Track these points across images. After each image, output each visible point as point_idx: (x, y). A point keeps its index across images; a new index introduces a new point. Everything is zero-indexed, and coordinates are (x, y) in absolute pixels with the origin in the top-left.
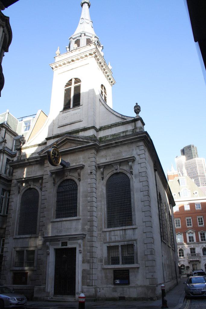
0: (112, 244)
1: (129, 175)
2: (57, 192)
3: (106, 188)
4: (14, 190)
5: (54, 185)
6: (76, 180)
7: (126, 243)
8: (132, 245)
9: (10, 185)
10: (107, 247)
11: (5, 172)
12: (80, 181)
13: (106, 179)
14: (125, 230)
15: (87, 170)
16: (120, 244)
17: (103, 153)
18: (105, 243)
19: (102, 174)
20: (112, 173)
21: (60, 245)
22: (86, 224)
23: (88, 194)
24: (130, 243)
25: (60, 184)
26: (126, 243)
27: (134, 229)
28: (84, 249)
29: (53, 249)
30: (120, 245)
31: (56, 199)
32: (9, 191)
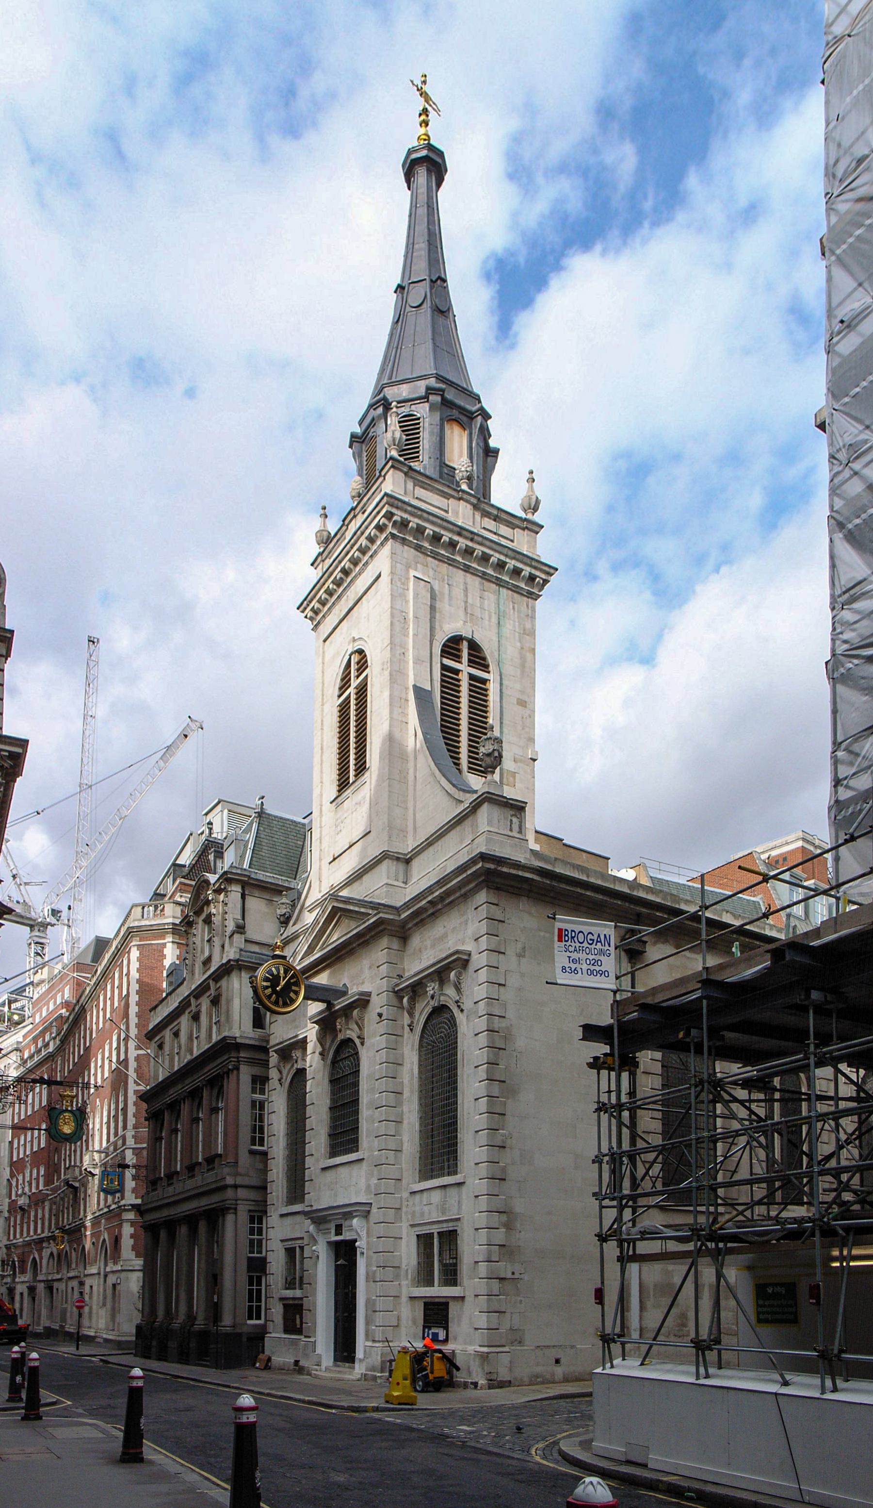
0: (425, 1230)
1: (455, 1010)
2: (331, 1081)
3: (420, 1060)
4: (273, 1074)
5: (323, 1059)
6: (357, 1041)
7: (445, 1225)
8: (456, 1231)
9: (265, 1064)
10: (418, 1236)
11: (258, 1022)
12: (362, 1044)
13: (419, 1029)
14: (445, 1187)
15: (378, 1003)
16: (435, 1229)
17: (416, 941)
18: (412, 1226)
19: (411, 1014)
20: (429, 1009)
21: (333, 1231)
22: (372, 1175)
23: (377, 1082)
24: (450, 1226)
25: (335, 1057)
26: (445, 1227)
27: (460, 1184)
28: (368, 1243)
29: (325, 1244)
30: (435, 1232)
31: (328, 1101)
32: (267, 1079)
